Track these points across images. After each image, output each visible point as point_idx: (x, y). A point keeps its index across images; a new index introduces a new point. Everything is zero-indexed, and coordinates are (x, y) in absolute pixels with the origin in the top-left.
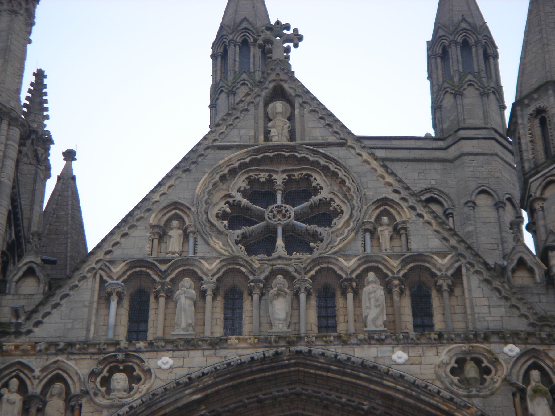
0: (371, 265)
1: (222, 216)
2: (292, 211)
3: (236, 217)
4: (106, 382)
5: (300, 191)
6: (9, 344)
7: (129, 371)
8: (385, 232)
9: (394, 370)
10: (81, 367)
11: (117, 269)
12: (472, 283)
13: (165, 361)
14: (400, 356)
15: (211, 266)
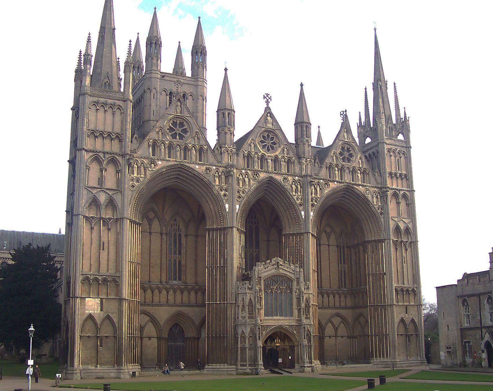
0: (194, 146)
1: (168, 129)
2: (180, 129)
3: (171, 129)
4: (150, 165)
5: (182, 125)
6: (135, 155)
7: (154, 163)
8: (196, 138)
9: (196, 170)
10: (146, 161)
11: (151, 141)
12: (209, 152)
13: (160, 163)
14: (197, 167)
15: (167, 143)
